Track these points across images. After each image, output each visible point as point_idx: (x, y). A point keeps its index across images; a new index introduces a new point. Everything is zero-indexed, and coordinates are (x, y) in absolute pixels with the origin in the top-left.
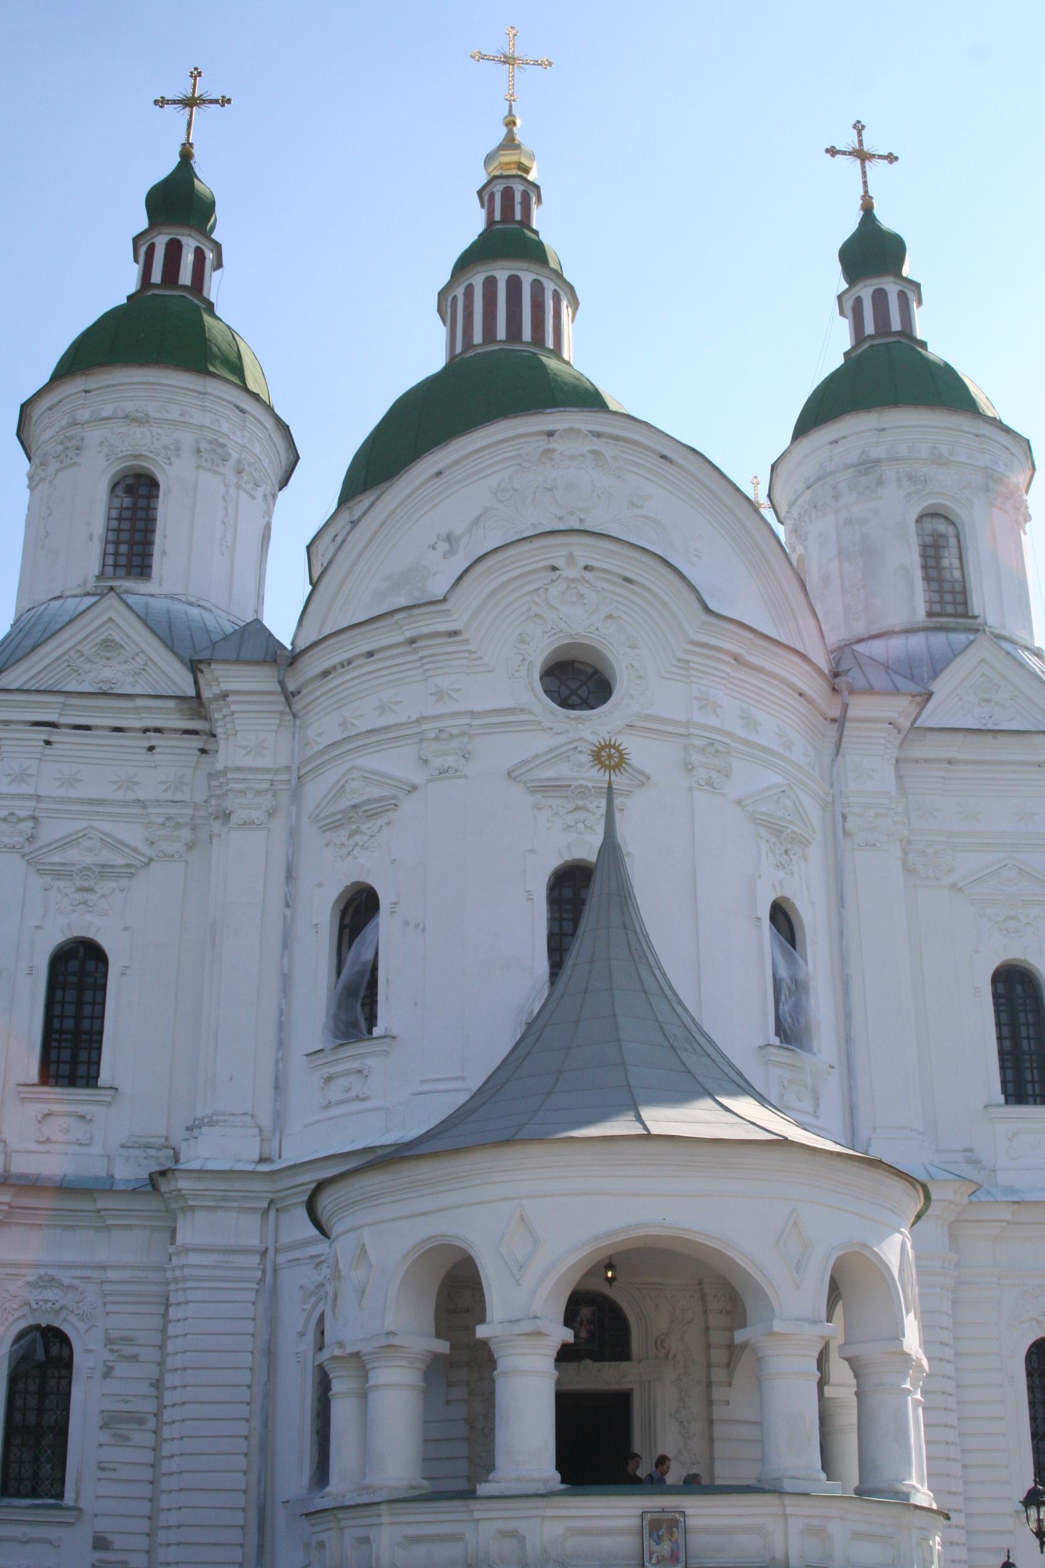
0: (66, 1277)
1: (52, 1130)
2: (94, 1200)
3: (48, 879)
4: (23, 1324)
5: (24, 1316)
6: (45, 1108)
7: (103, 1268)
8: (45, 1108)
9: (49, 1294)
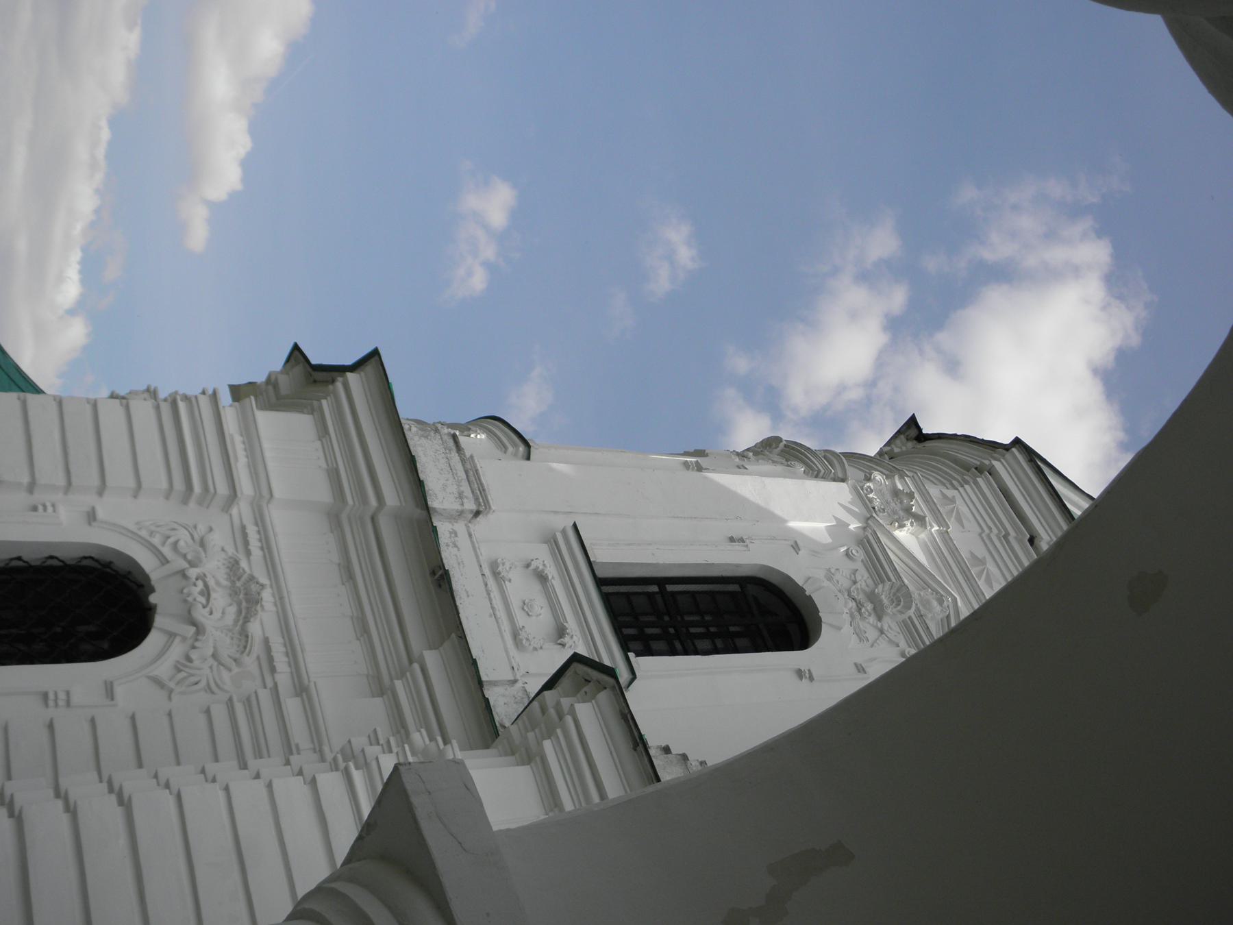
0: (264, 624)
1: (520, 587)
2: (431, 647)
3: (859, 554)
4: (146, 561)
5: (165, 561)
6: (551, 571)
7: (302, 690)
8: (551, 571)
9: (220, 599)
